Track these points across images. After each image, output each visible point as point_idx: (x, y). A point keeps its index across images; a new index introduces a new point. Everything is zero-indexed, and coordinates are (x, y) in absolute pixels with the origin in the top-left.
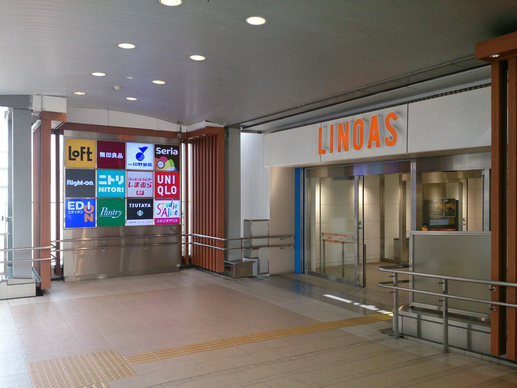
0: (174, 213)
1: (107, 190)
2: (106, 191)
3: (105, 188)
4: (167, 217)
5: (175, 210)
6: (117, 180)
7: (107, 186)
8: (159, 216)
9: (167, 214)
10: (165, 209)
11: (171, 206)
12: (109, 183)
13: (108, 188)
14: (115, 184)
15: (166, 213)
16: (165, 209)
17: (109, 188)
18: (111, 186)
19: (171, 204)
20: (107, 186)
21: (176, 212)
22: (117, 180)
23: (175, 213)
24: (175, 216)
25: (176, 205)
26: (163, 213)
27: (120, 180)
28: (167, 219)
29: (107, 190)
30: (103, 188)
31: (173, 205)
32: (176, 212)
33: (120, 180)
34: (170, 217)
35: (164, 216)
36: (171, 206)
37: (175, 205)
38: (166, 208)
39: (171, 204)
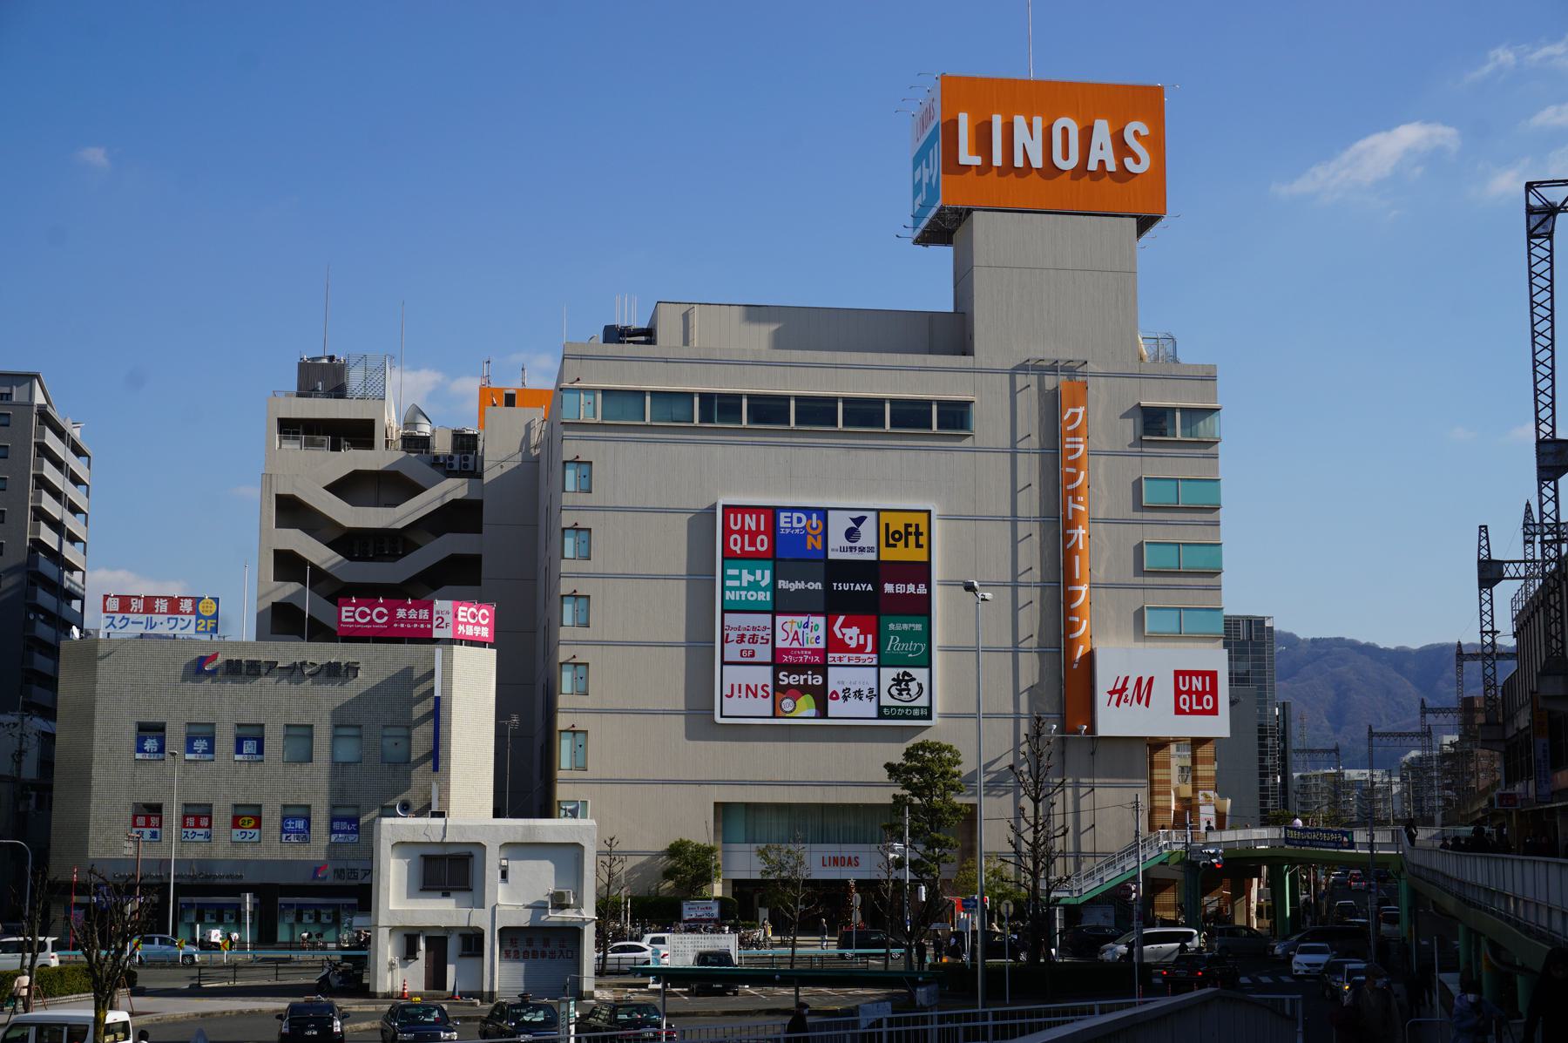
0: (814, 640)
1: (741, 595)
2: (738, 598)
3: (737, 592)
4: (798, 646)
5: (815, 634)
6: (758, 577)
7: (740, 588)
8: (786, 645)
9: (801, 641)
10: (796, 633)
11: (807, 627)
12: (745, 584)
13: (741, 592)
14: (754, 586)
15: (798, 639)
16: (796, 633)
17: (743, 593)
18: (747, 589)
19: (807, 623)
20: (740, 588)
21: (818, 638)
22: (758, 577)
23: (816, 639)
24: (815, 646)
25: (817, 625)
26: (793, 639)
27: (763, 578)
28: (800, 649)
29: (741, 595)
30: (733, 592)
31: (810, 625)
32: (818, 638)
33: (763, 578)
34: (806, 646)
35: (795, 645)
36: (807, 627)
37: (814, 625)
38: (798, 630)
39: (807, 623)
